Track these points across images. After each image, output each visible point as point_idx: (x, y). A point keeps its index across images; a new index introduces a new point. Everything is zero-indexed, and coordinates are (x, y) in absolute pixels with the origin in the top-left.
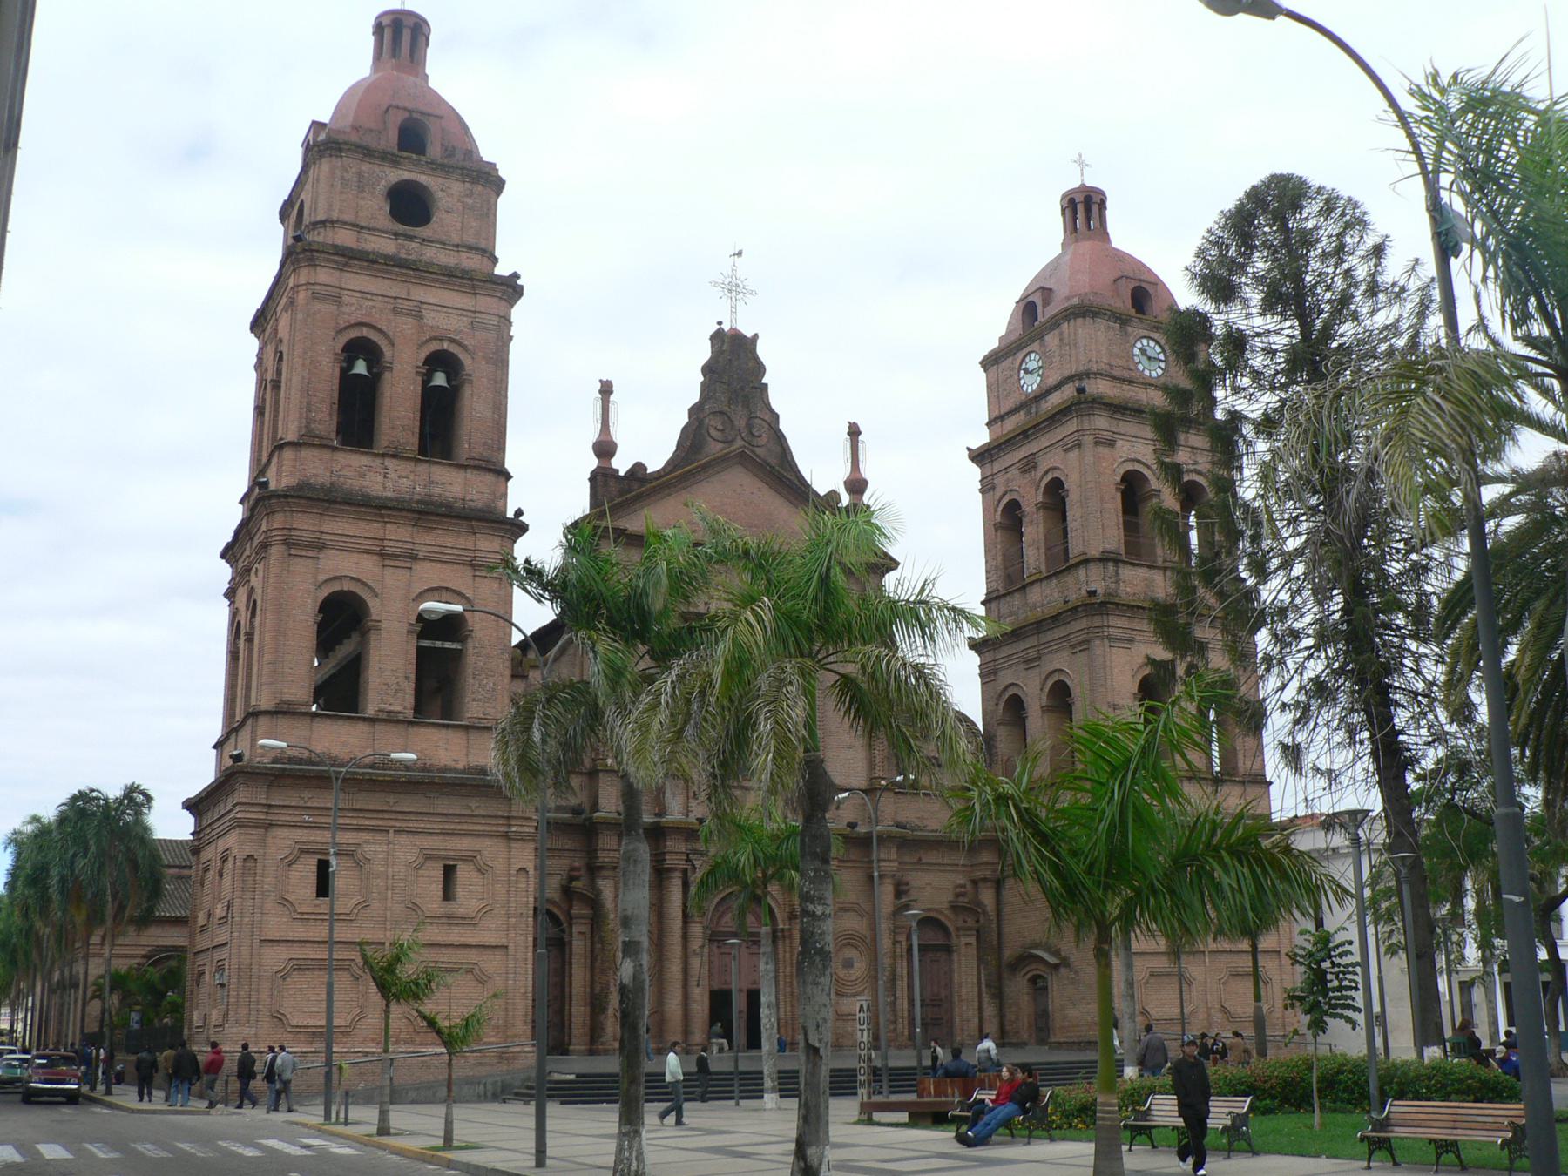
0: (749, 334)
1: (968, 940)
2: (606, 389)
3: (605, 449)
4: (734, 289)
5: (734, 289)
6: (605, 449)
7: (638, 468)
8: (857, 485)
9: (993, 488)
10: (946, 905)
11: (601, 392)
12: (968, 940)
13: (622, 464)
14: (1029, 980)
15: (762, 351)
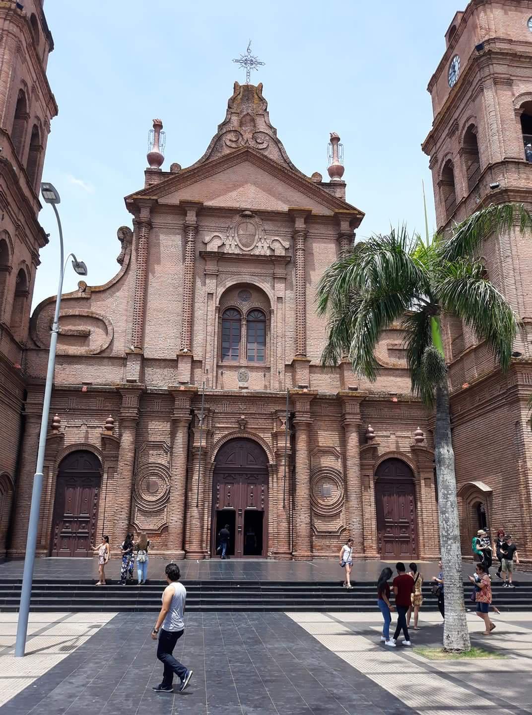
0: (256, 85)
1: (427, 475)
2: (158, 126)
3: (155, 159)
4: (249, 62)
5: (249, 62)
6: (155, 159)
7: (175, 166)
8: (337, 171)
9: (437, 161)
10: (408, 449)
11: (155, 126)
12: (427, 475)
13: (165, 168)
14: (474, 506)
15: (264, 94)
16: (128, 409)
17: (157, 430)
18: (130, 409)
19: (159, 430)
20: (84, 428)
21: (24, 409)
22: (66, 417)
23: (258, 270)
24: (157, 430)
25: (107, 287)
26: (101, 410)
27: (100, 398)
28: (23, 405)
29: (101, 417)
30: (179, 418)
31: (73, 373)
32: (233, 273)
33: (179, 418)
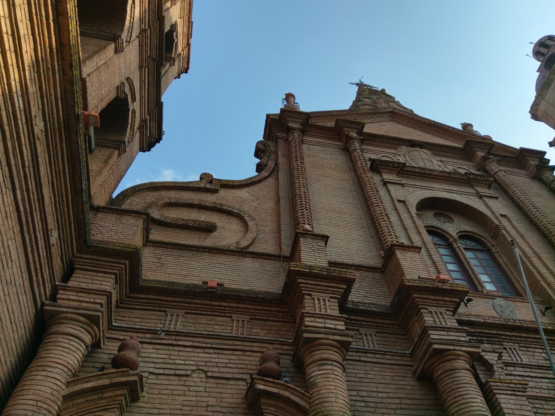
16: (322, 320)
17: (385, 395)
18: (327, 321)
19: (390, 395)
20: (199, 380)
21: (54, 298)
22: (155, 351)
23: (455, 188)
24: (385, 395)
25: (245, 182)
26: (244, 340)
27: (241, 317)
28: (55, 290)
29: (242, 357)
30: (452, 347)
31: (184, 273)
32: (421, 188)
33: (452, 347)
